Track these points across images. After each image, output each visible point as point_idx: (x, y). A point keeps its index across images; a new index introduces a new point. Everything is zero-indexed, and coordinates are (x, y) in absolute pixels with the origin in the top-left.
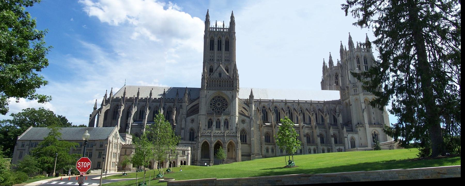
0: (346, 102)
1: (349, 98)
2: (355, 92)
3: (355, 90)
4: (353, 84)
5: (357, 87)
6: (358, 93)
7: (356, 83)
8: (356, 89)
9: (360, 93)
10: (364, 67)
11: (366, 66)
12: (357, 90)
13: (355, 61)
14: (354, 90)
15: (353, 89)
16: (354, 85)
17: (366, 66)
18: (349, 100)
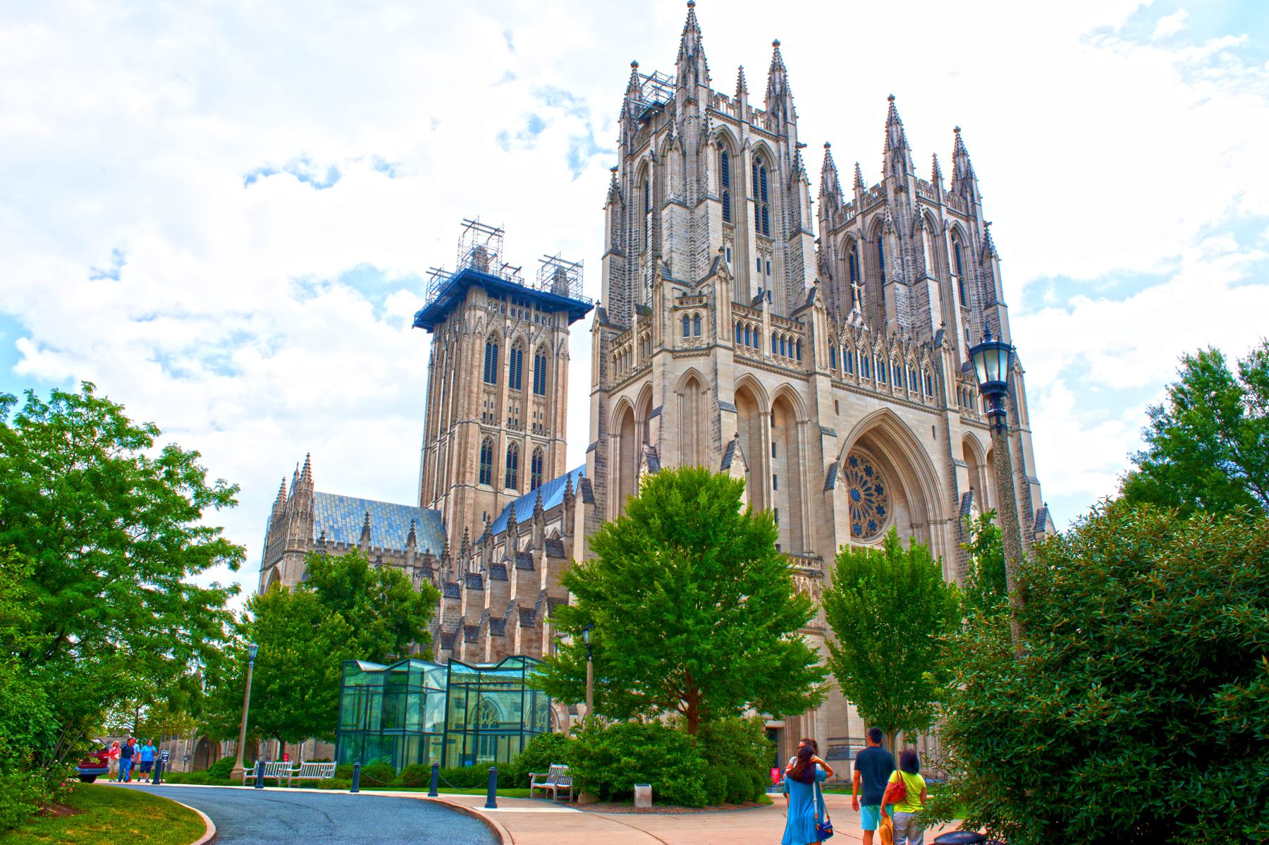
0: (624, 402)
1: (648, 369)
2: (686, 334)
3: (691, 323)
4: (684, 289)
5: (706, 306)
6: (705, 339)
7: (699, 283)
8: (697, 316)
9: (719, 342)
10: (751, 206)
11: (761, 205)
12: (704, 322)
13: (711, 156)
14: (686, 319)
15: (679, 314)
16: (685, 294)
17: (761, 205)
18: (647, 391)
